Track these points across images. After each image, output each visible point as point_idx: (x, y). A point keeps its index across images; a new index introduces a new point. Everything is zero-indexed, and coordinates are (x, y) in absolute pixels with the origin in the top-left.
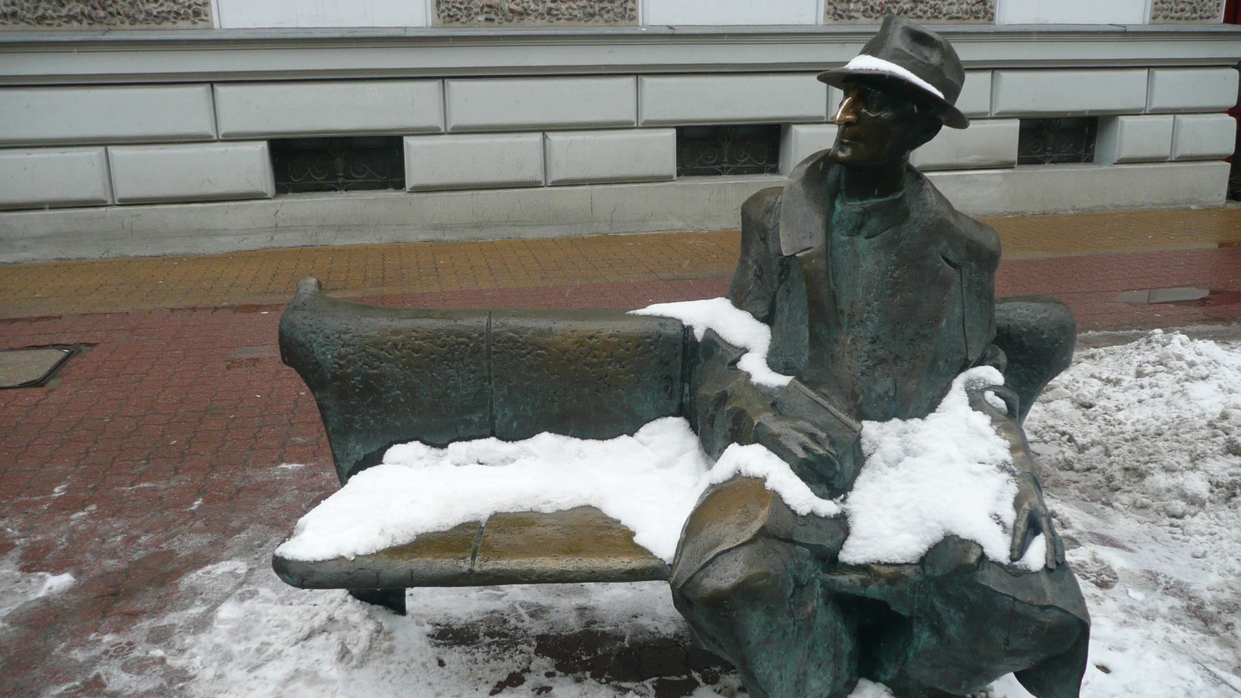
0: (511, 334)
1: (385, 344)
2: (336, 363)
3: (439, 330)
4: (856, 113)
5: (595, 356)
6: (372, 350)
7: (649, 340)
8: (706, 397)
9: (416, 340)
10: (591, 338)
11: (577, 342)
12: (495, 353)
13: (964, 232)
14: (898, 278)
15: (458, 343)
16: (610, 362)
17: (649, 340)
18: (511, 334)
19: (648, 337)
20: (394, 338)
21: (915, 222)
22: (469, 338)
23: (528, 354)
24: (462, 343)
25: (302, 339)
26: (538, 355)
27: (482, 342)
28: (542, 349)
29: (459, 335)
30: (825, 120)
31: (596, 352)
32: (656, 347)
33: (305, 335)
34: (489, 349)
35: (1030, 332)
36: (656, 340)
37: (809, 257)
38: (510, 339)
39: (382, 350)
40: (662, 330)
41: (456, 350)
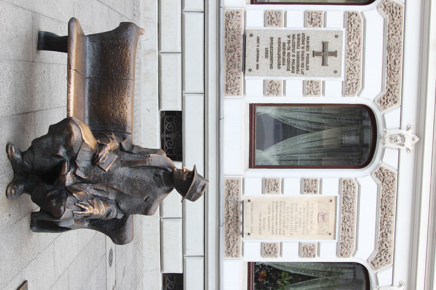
0: (128, 86)
1: (127, 51)
2: (122, 37)
3: (130, 66)
4: (185, 172)
5: (121, 108)
6: (125, 48)
7: (125, 123)
8: (112, 134)
9: (128, 60)
10: (126, 107)
11: (125, 103)
12: (123, 81)
13: (155, 203)
14: (143, 184)
15: (126, 71)
16: (120, 112)
17: (125, 123)
18: (128, 86)
19: (126, 123)
20: (128, 54)
21: (158, 190)
22: (128, 74)
23: (123, 90)
24: (126, 72)
25: (129, 29)
26: (122, 92)
27: (126, 78)
28: (124, 93)
29: (129, 71)
30: (184, 256)
31: (122, 108)
32: (123, 125)
33: (130, 30)
34: (125, 79)
35: (125, 230)
36: (125, 125)
37: (149, 160)
38: (127, 85)
39: (125, 50)
40: (128, 127)
41: (125, 70)
